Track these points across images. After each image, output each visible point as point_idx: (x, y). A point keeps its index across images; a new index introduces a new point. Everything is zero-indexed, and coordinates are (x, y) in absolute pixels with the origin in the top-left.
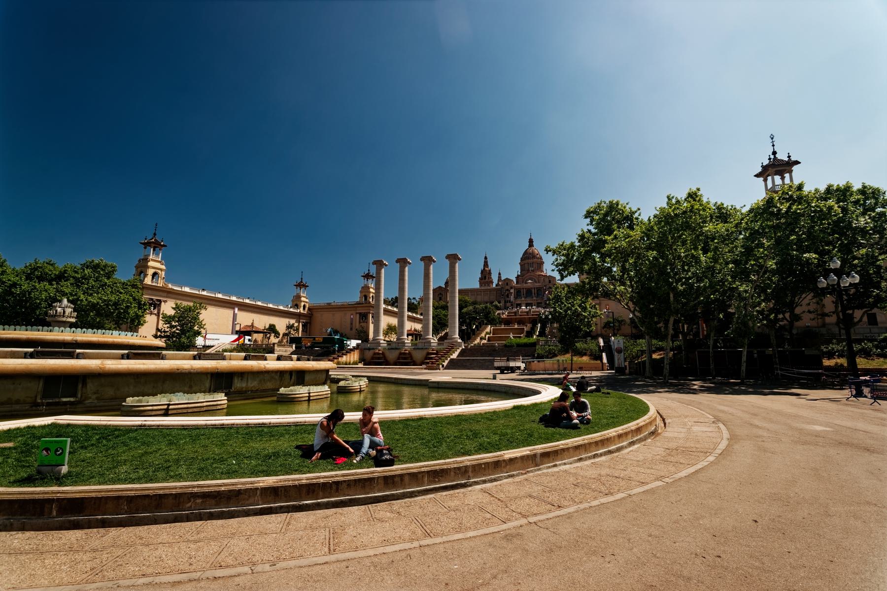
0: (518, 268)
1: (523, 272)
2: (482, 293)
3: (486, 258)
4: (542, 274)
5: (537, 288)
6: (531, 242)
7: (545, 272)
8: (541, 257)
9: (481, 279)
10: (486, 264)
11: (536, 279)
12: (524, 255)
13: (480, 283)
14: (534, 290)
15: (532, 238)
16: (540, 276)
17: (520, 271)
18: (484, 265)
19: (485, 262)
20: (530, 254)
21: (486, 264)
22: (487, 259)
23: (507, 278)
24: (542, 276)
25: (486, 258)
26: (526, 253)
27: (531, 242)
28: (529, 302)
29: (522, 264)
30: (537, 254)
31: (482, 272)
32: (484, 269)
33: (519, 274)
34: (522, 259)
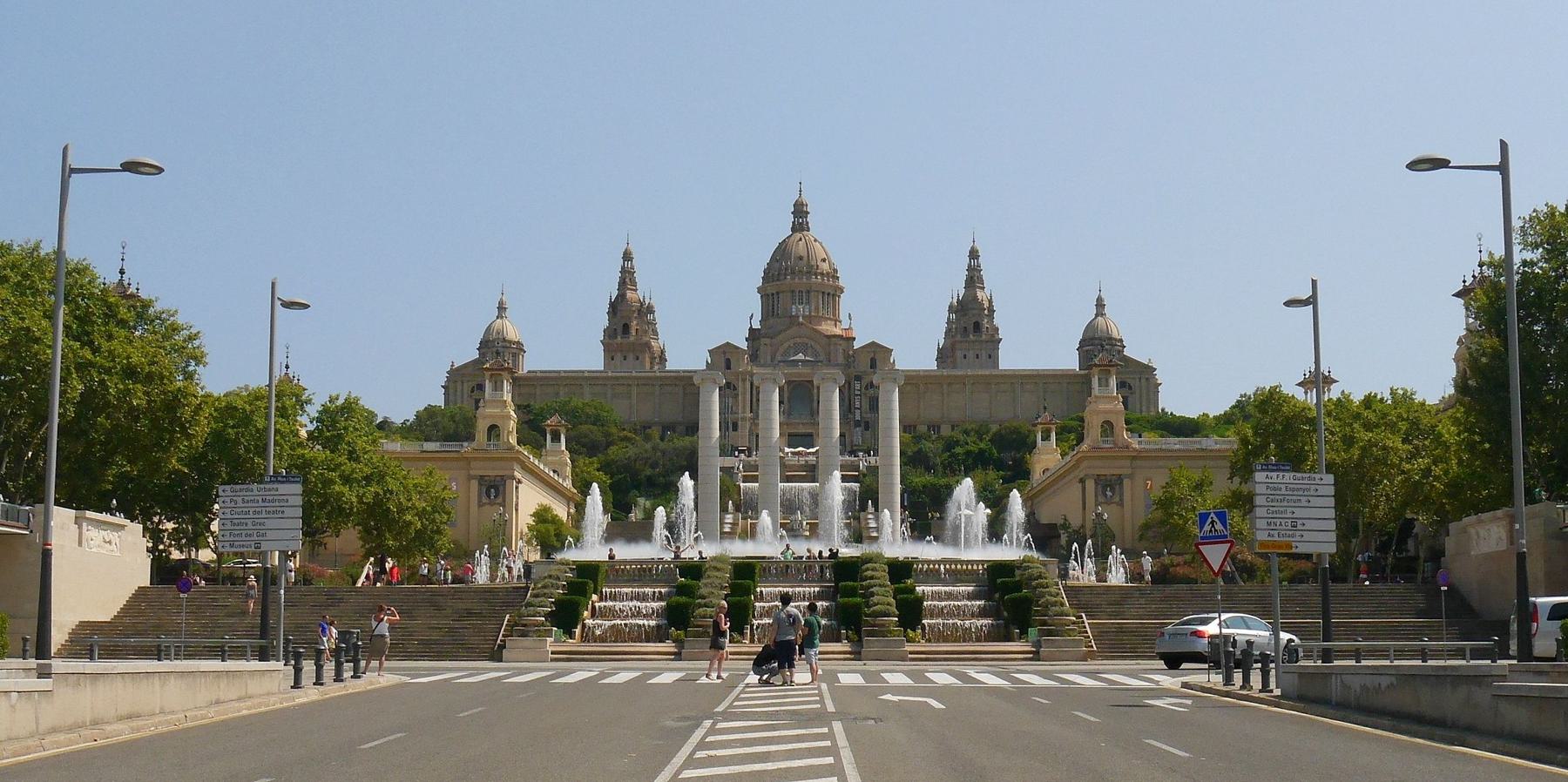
0: (755, 306)
1: (771, 321)
2: (635, 390)
4: (838, 331)
6: (800, 211)
8: (836, 271)
9: (610, 333)
10: (627, 278)
11: (818, 347)
15: (805, 198)
17: (758, 317)
18: (623, 284)
19: (623, 271)
20: (801, 258)
22: (631, 259)
26: (782, 251)
27: (800, 211)
28: (802, 430)
29: (769, 291)
30: (824, 260)
32: (622, 295)
33: (756, 325)
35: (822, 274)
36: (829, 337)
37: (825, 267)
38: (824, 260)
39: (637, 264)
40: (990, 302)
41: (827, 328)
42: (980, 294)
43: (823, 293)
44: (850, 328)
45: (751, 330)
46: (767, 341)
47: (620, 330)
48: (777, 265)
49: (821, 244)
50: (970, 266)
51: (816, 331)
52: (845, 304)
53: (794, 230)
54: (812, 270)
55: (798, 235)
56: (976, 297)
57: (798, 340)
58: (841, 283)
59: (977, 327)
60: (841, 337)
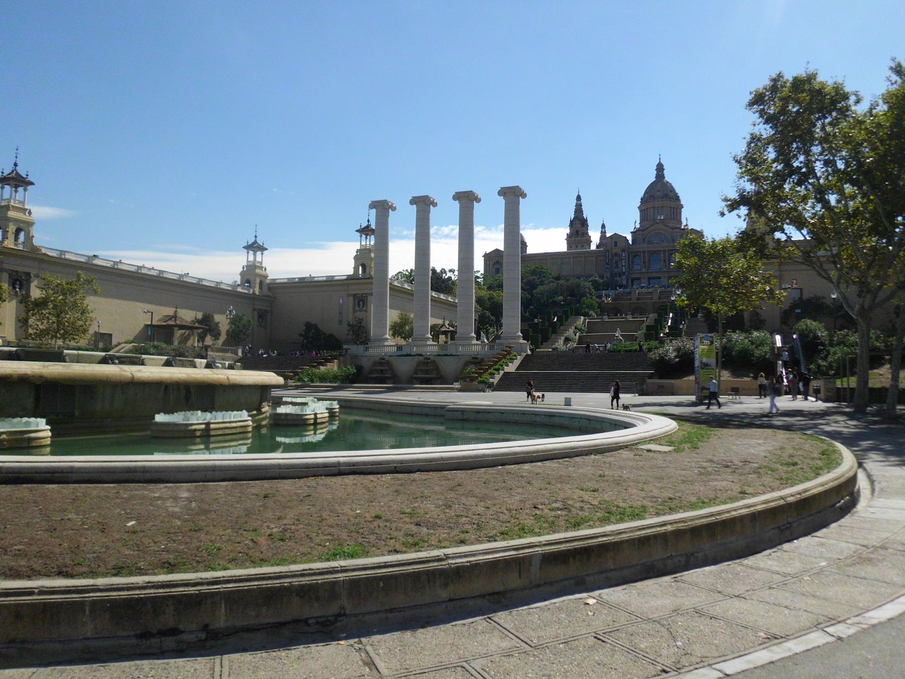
3: (579, 198)
6: (660, 168)
10: (579, 210)
13: (568, 244)
14: (664, 254)
17: (638, 222)
21: (579, 210)
25: (579, 198)
27: (660, 168)
29: (643, 209)
31: (572, 224)
33: (638, 226)
34: (643, 200)
36: (673, 229)
37: (672, 194)
38: (671, 191)
39: (583, 202)
43: (671, 207)
44: (687, 225)
48: (647, 195)
57: (657, 231)
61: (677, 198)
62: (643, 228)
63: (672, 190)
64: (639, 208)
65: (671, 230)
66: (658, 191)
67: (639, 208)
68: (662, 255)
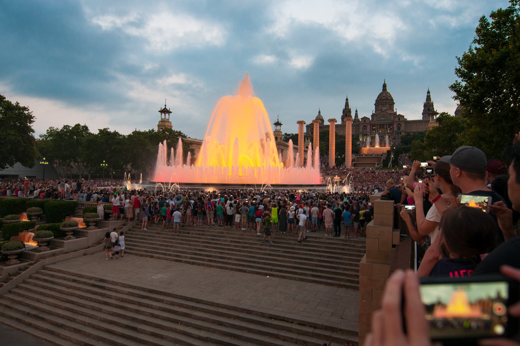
0: (373, 108)
3: (347, 100)
4: (393, 112)
5: (388, 124)
6: (385, 86)
7: (395, 111)
10: (347, 104)
11: (387, 117)
12: (378, 97)
16: (391, 115)
17: (374, 111)
20: (384, 97)
21: (347, 104)
23: (365, 117)
24: (392, 115)
25: (347, 100)
27: (385, 86)
29: (377, 104)
30: (390, 97)
31: (344, 111)
32: (345, 108)
33: (374, 112)
34: (377, 101)
35: (389, 100)
36: (390, 114)
37: (390, 98)
38: (390, 97)
40: (433, 103)
41: (389, 112)
42: (430, 102)
45: (373, 113)
46: (376, 116)
47: (345, 116)
48: (379, 99)
49: (389, 93)
50: (427, 95)
51: (387, 113)
52: (395, 106)
53: (383, 90)
54: (387, 99)
55: (384, 91)
56: (429, 103)
58: (394, 102)
59: (429, 109)
60: (393, 114)
61: (392, 100)
62: (377, 114)
63: (390, 96)
64: (375, 104)
65: (389, 115)
66: (384, 97)
67: (375, 104)
68: (385, 126)
